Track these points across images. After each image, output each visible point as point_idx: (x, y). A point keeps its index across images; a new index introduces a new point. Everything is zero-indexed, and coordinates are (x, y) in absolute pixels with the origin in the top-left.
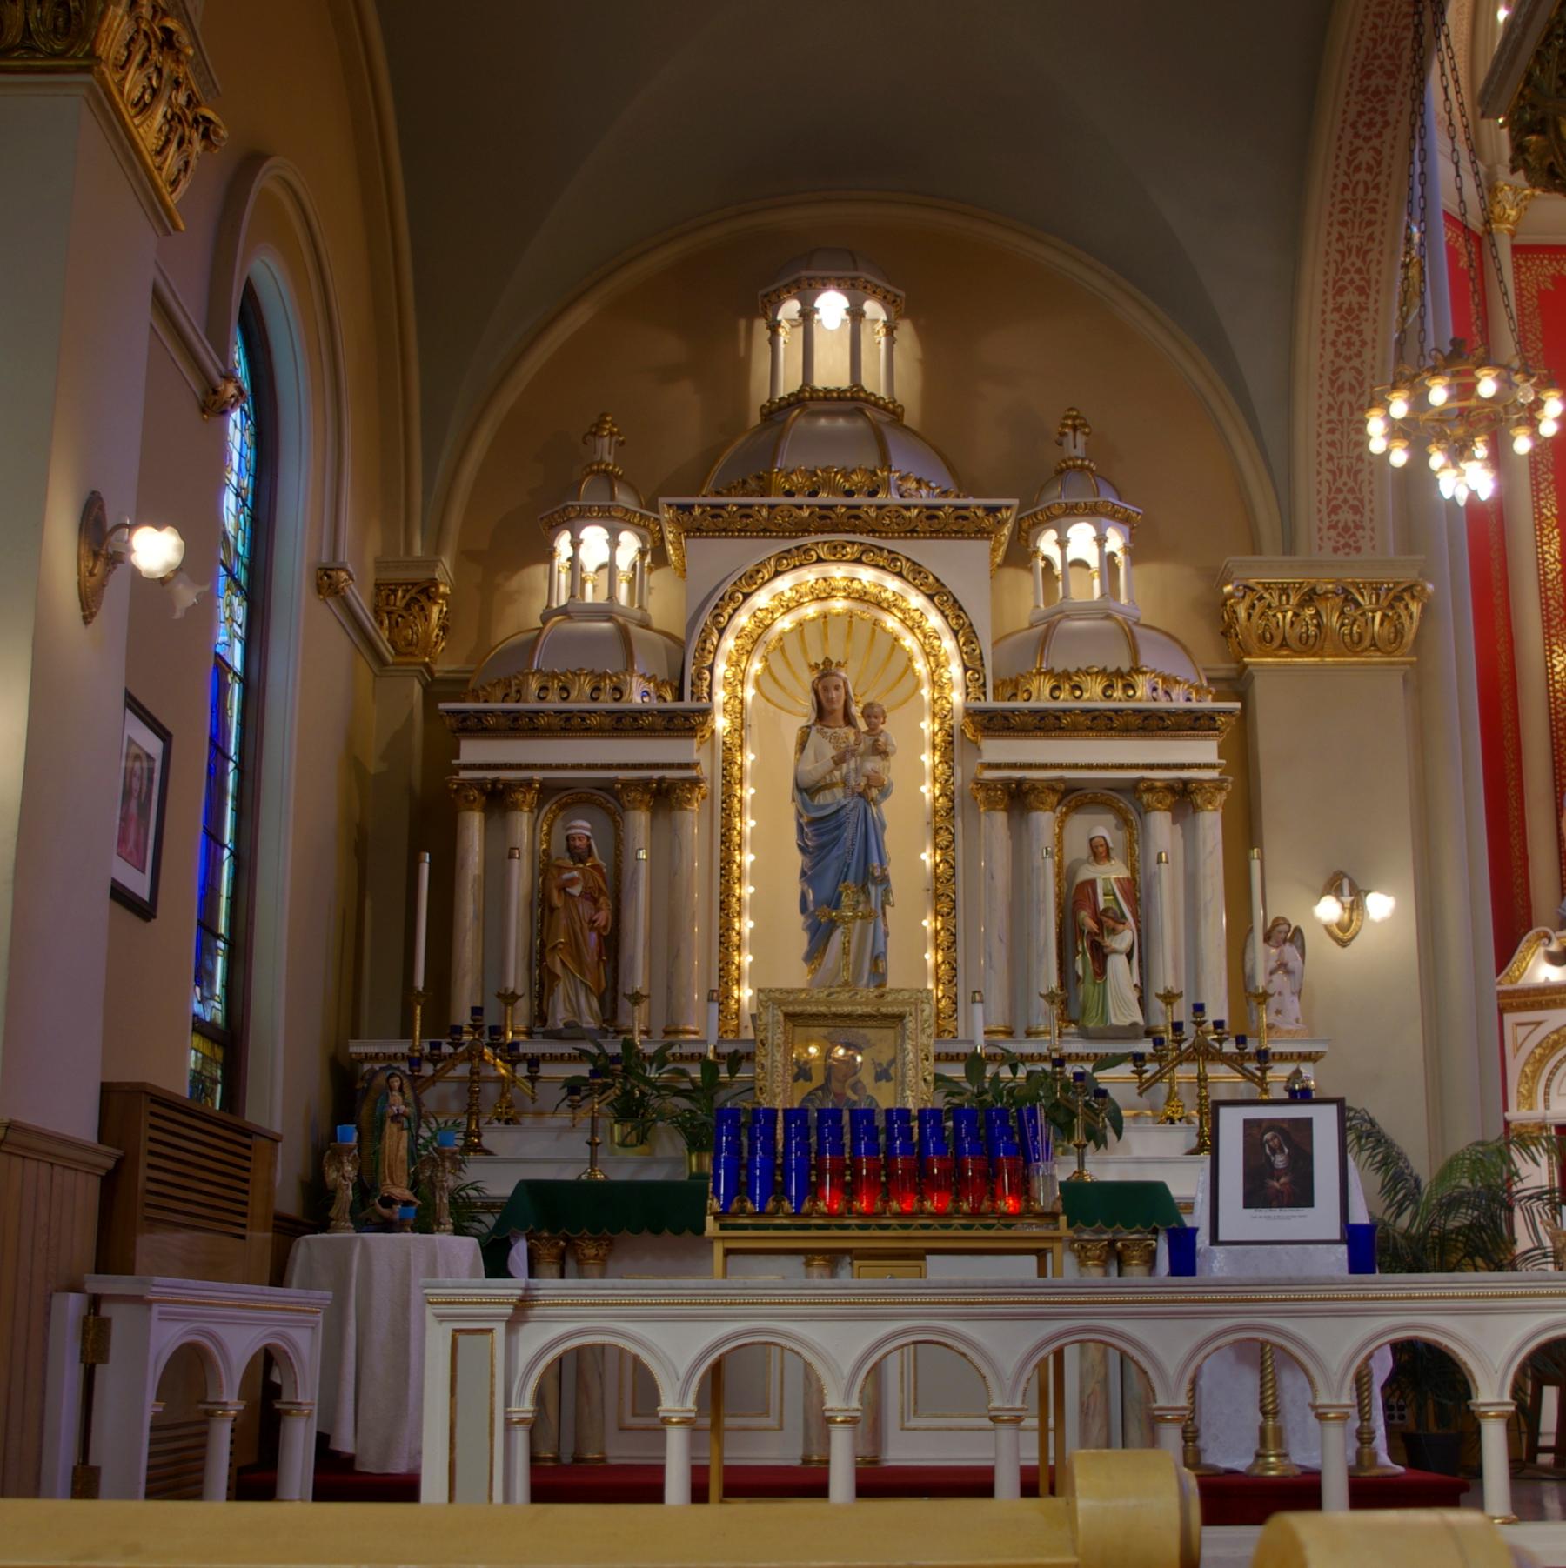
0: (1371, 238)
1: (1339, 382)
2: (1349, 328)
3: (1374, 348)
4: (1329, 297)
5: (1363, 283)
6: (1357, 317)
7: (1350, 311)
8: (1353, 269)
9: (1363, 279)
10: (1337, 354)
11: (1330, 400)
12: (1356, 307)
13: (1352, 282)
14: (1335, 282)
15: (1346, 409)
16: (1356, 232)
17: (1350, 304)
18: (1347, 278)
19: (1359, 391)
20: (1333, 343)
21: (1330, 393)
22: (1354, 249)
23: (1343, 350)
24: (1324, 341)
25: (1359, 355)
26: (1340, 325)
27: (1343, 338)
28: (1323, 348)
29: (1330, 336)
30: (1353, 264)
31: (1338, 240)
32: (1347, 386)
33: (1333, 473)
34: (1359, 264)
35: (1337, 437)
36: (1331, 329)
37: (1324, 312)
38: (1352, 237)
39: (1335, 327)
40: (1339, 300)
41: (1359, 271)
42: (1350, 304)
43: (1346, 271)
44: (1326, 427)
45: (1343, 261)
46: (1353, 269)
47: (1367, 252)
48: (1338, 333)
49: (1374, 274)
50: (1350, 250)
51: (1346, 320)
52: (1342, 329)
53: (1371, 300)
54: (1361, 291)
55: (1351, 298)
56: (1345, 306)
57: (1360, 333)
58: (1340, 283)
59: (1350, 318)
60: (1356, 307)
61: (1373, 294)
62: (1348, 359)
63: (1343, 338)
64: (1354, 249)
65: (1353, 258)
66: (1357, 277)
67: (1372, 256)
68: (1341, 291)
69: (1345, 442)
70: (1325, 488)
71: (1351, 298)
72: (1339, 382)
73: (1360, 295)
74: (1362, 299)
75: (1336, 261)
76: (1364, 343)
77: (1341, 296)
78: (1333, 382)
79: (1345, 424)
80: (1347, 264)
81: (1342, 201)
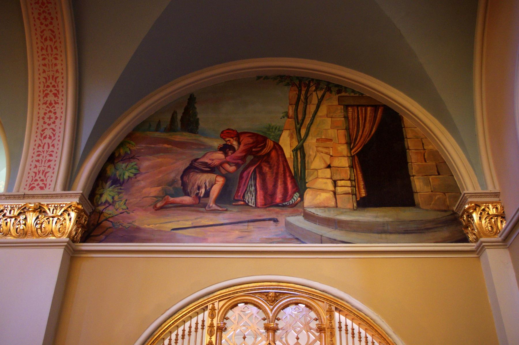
0: (57, 71)
1: (44, 135)
2: (50, 111)
3: (61, 119)
4: (41, 98)
5: (56, 92)
6: (54, 107)
7: (51, 104)
8: (51, 86)
9: (56, 90)
10: (45, 123)
11: (40, 142)
12: (53, 102)
13: (51, 91)
14: (44, 91)
15: (46, 146)
16: (51, 69)
17: (51, 101)
18: (49, 89)
19: (53, 138)
20: (43, 118)
21: (40, 140)
22: (51, 77)
23: (47, 120)
24: (39, 117)
25: (54, 123)
26: (46, 110)
27: (47, 116)
28: (39, 120)
29: (42, 115)
30: (51, 83)
31: (43, 73)
32: (48, 136)
33: (36, 173)
34: (54, 83)
35: (40, 158)
36: (42, 112)
37: (39, 105)
38: (49, 71)
39: (44, 111)
40: (46, 99)
41: (54, 86)
42: (51, 101)
43: (48, 86)
44: (36, 154)
45: (46, 82)
46: (51, 86)
47: (57, 78)
48: (45, 114)
49: (60, 88)
50: (49, 77)
51: (49, 108)
52: (47, 112)
53: (60, 100)
54: (55, 95)
55: (51, 98)
56: (48, 103)
57: (55, 113)
58: (46, 92)
59: (50, 107)
60: (53, 102)
61: (60, 96)
62: (49, 125)
63: (47, 116)
64: (51, 77)
65: (51, 80)
66: (53, 89)
67: (59, 79)
68: (46, 95)
69: (44, 160)
70: (30, 180)
71: (51, 98)
72: (44, 135)
73: (55, 97)
74: (56, 99)
75: (43, 82)
76: (56, 118)
77: (47, 97)
78: (42, 135)
79: (45, 152)
80: (48, 83)
81: (43, 55)
